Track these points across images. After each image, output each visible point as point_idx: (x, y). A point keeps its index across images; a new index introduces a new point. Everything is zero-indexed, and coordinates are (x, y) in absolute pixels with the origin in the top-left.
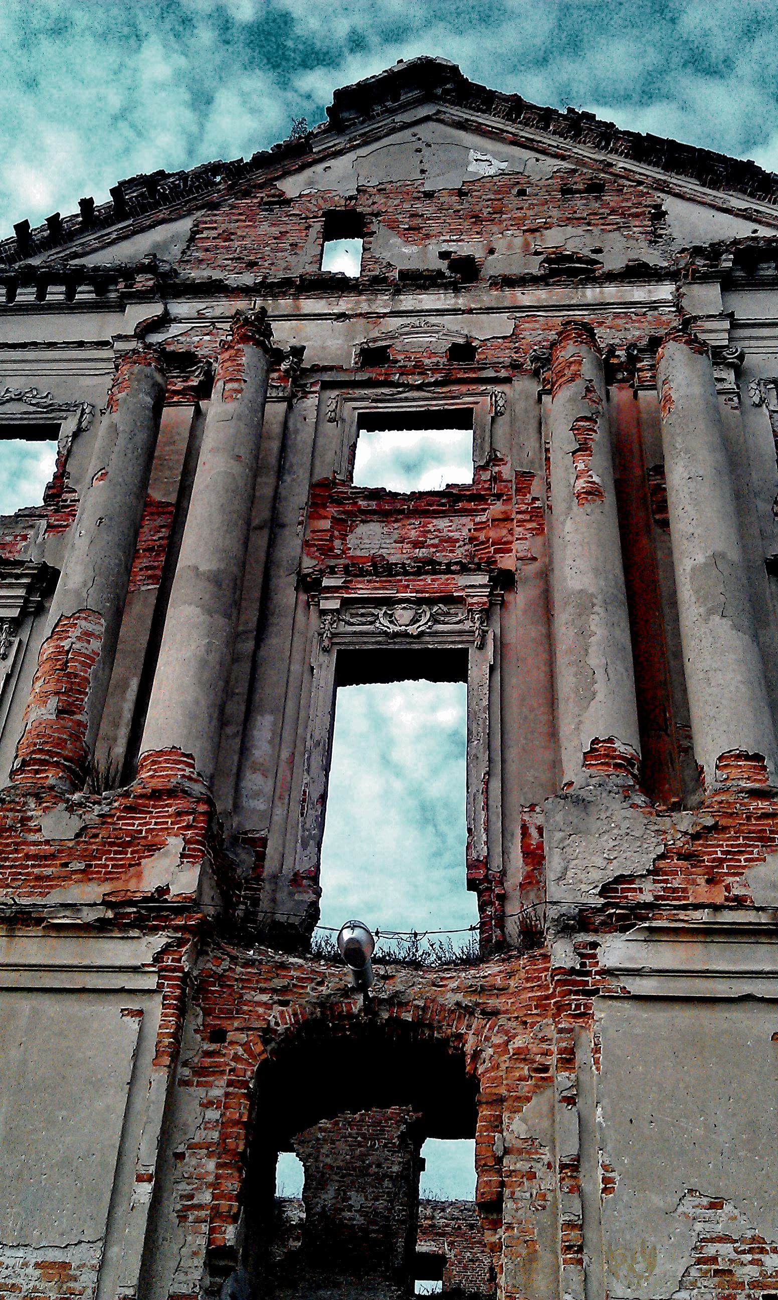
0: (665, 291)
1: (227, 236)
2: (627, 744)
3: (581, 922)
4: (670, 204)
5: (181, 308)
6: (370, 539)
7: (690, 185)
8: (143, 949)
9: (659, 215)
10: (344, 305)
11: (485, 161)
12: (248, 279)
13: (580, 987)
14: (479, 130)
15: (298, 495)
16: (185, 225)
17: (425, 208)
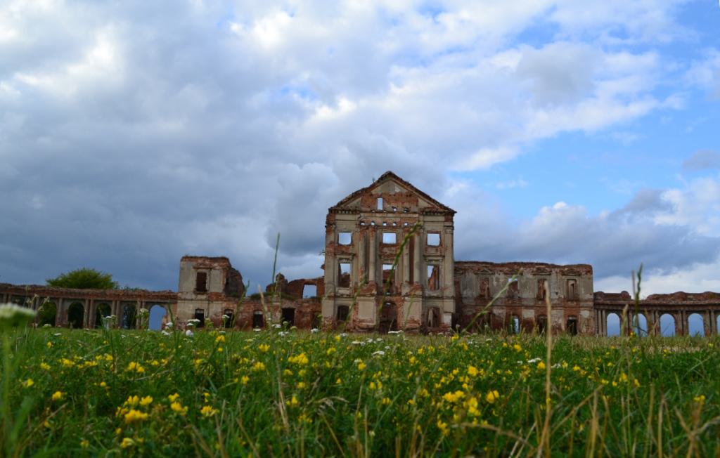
0: (417, 215)
1: (366, 201)
2: (408, 280)
3: (404, 296)
4: (420, 200)
5: (362, 214)
6: (386, 250)
7: (422, 197)
8: (373, 298)
9: (418, 201)
10: (381, 215)
11: (398, 190)
12: (369, 210)
13: (404, 301)
14: (397, 183)
15: (378, 245)
16: (360, 199)
17: (390, 197)
